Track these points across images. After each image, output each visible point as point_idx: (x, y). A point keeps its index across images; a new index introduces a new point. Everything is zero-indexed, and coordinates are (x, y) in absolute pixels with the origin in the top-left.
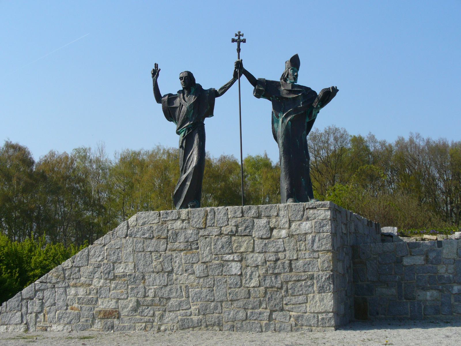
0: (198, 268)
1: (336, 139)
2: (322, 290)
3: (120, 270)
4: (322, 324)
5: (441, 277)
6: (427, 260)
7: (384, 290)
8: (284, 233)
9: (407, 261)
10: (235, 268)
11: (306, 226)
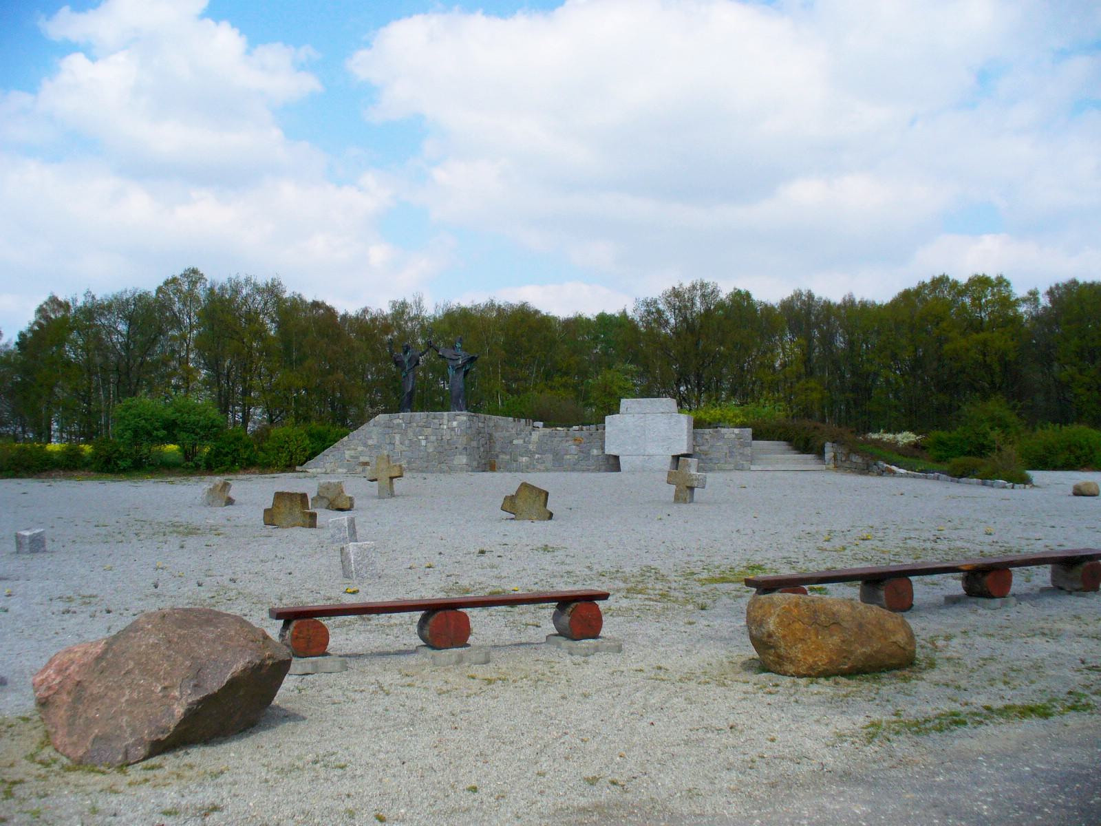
0: (407, 442)
1: (703, 296)
2: (461, 454)
3: (370, 442)
4: (462, 470)
5: (530, 451)
6: (524, 442)
7: (504, 457)
8: (445, 427)
9: (515, 442)
10: (423, 443)
11: (455, 424)
